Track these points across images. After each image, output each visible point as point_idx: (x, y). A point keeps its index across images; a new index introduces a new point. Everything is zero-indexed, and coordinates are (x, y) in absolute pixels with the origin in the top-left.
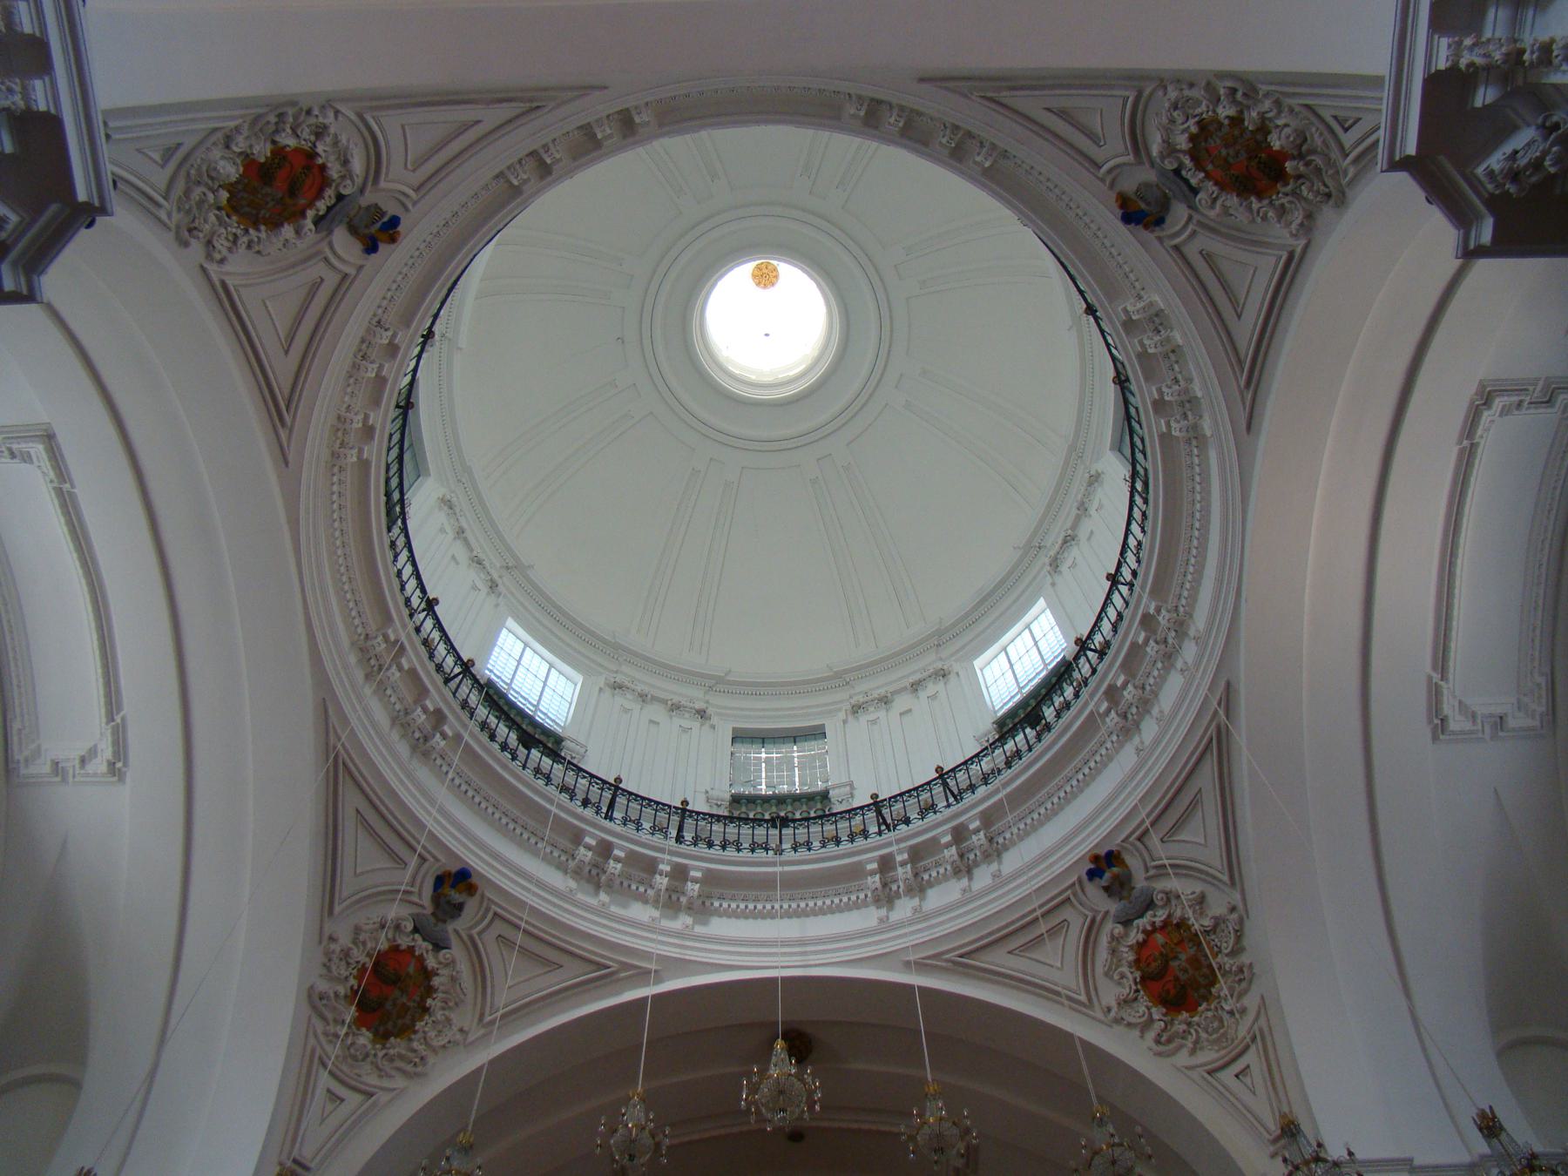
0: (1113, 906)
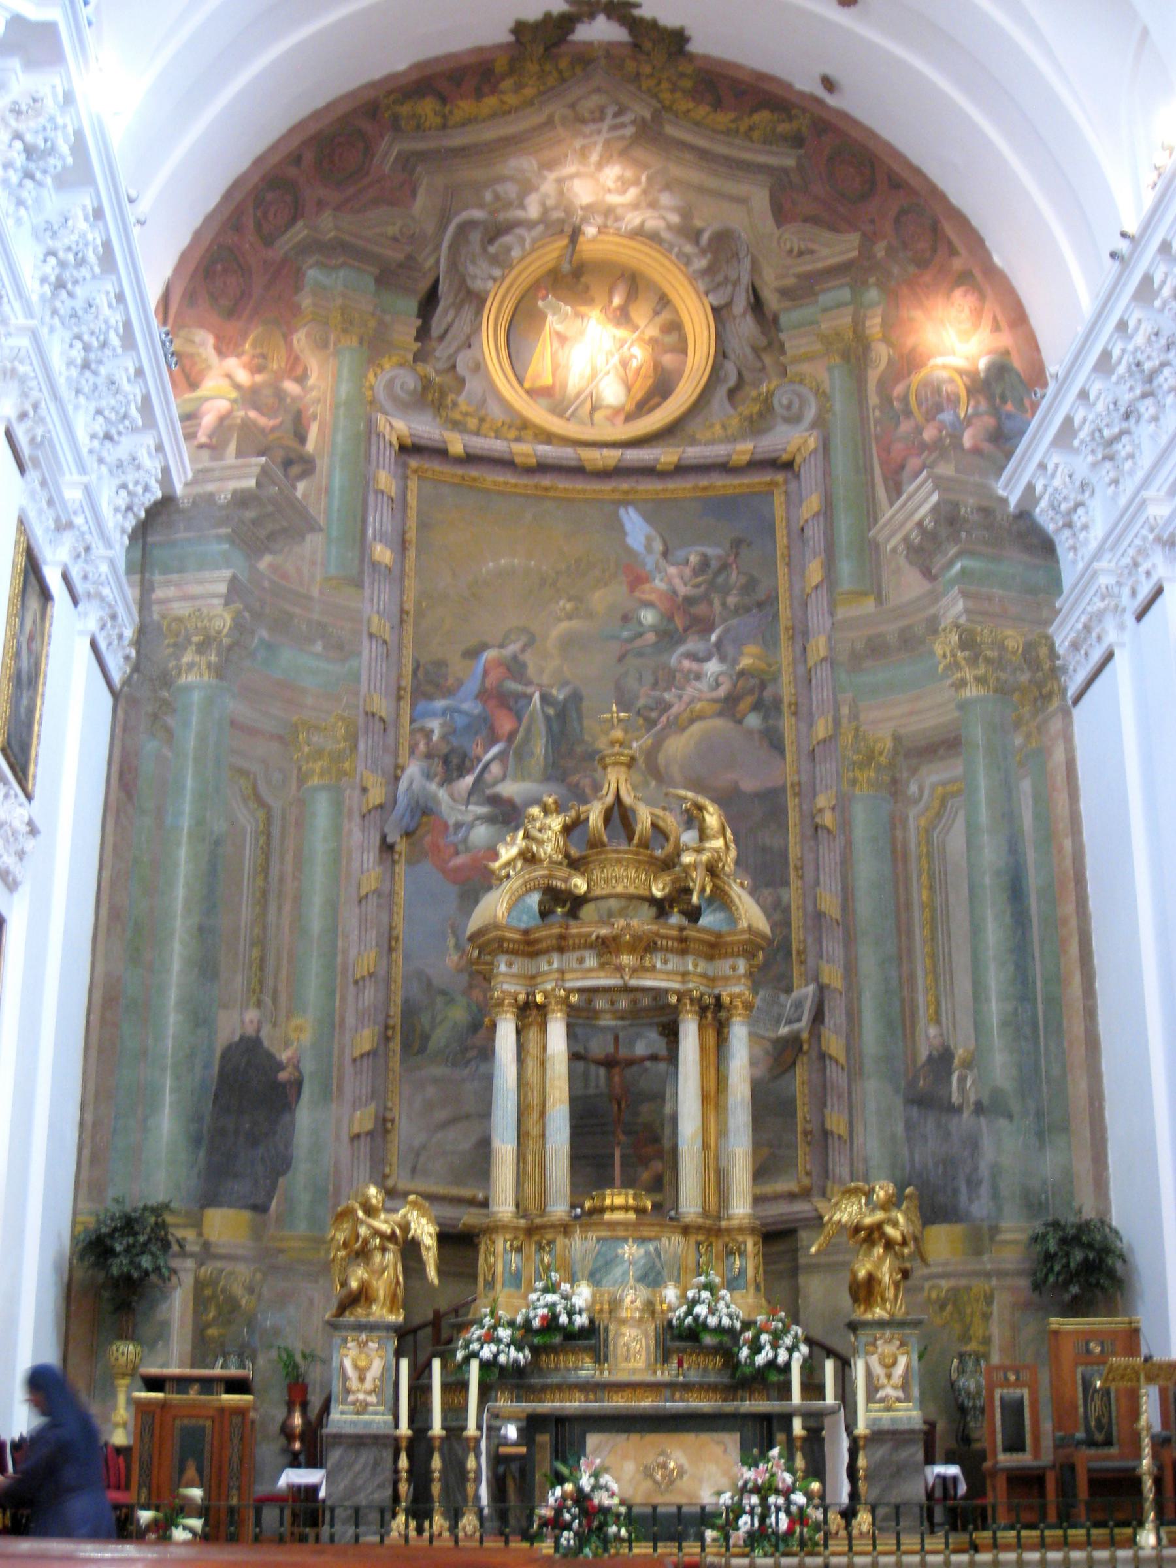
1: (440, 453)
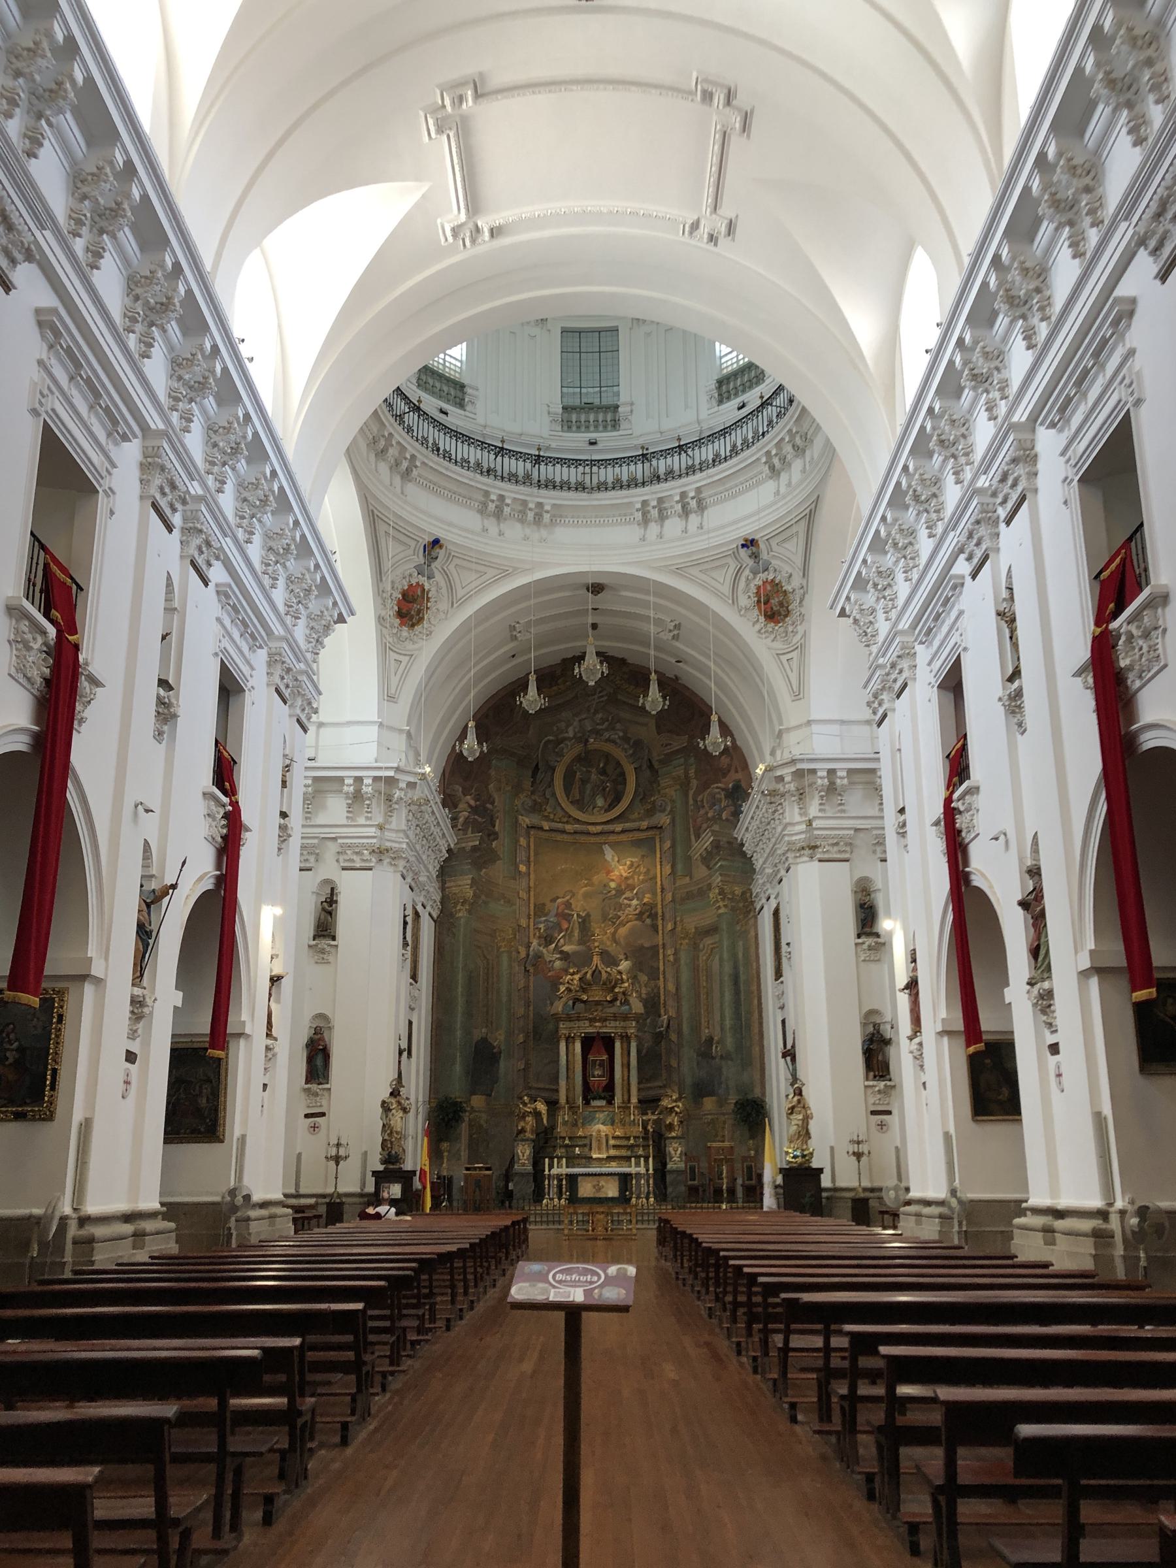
0: (751, 562)
1: (541, 828)
